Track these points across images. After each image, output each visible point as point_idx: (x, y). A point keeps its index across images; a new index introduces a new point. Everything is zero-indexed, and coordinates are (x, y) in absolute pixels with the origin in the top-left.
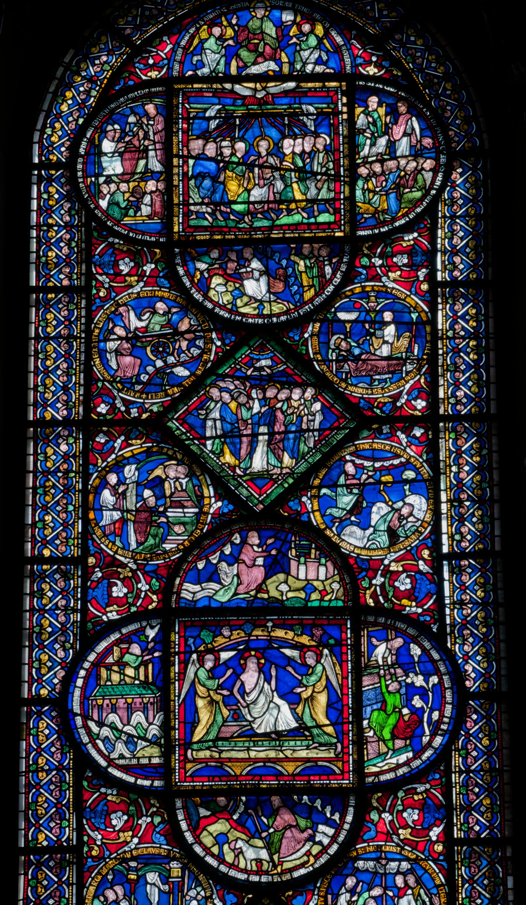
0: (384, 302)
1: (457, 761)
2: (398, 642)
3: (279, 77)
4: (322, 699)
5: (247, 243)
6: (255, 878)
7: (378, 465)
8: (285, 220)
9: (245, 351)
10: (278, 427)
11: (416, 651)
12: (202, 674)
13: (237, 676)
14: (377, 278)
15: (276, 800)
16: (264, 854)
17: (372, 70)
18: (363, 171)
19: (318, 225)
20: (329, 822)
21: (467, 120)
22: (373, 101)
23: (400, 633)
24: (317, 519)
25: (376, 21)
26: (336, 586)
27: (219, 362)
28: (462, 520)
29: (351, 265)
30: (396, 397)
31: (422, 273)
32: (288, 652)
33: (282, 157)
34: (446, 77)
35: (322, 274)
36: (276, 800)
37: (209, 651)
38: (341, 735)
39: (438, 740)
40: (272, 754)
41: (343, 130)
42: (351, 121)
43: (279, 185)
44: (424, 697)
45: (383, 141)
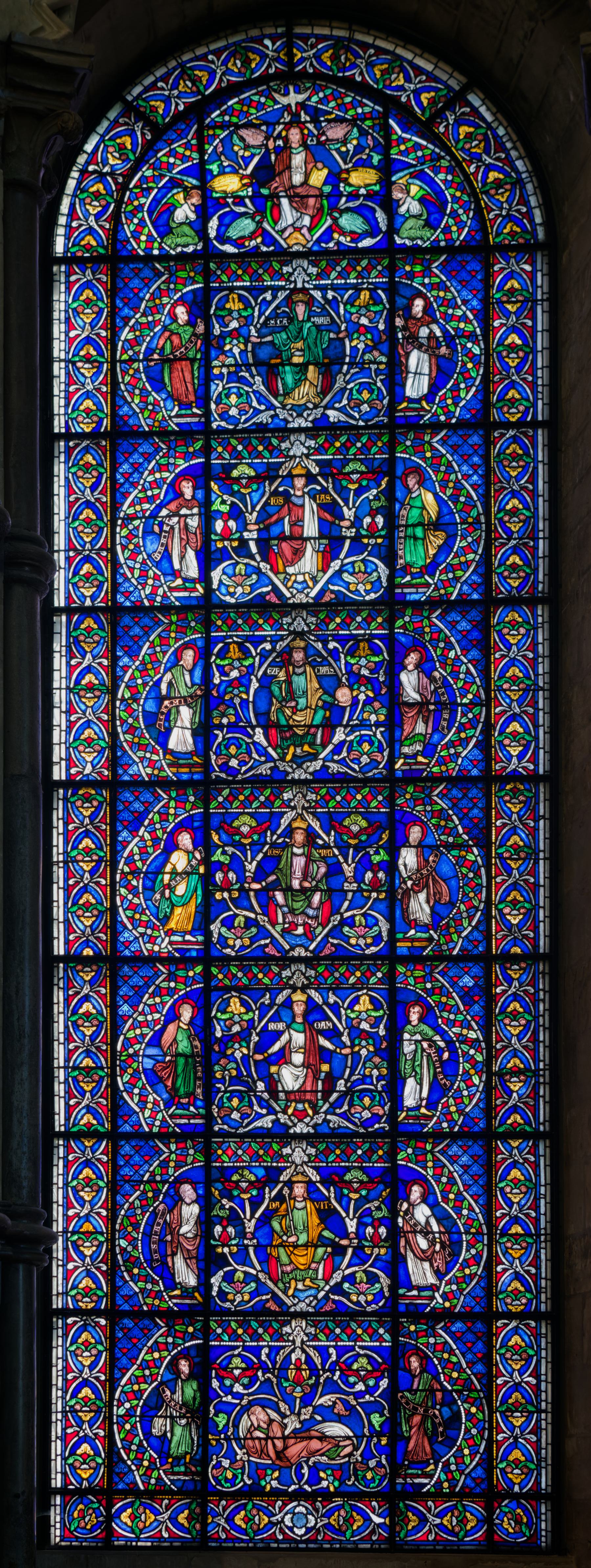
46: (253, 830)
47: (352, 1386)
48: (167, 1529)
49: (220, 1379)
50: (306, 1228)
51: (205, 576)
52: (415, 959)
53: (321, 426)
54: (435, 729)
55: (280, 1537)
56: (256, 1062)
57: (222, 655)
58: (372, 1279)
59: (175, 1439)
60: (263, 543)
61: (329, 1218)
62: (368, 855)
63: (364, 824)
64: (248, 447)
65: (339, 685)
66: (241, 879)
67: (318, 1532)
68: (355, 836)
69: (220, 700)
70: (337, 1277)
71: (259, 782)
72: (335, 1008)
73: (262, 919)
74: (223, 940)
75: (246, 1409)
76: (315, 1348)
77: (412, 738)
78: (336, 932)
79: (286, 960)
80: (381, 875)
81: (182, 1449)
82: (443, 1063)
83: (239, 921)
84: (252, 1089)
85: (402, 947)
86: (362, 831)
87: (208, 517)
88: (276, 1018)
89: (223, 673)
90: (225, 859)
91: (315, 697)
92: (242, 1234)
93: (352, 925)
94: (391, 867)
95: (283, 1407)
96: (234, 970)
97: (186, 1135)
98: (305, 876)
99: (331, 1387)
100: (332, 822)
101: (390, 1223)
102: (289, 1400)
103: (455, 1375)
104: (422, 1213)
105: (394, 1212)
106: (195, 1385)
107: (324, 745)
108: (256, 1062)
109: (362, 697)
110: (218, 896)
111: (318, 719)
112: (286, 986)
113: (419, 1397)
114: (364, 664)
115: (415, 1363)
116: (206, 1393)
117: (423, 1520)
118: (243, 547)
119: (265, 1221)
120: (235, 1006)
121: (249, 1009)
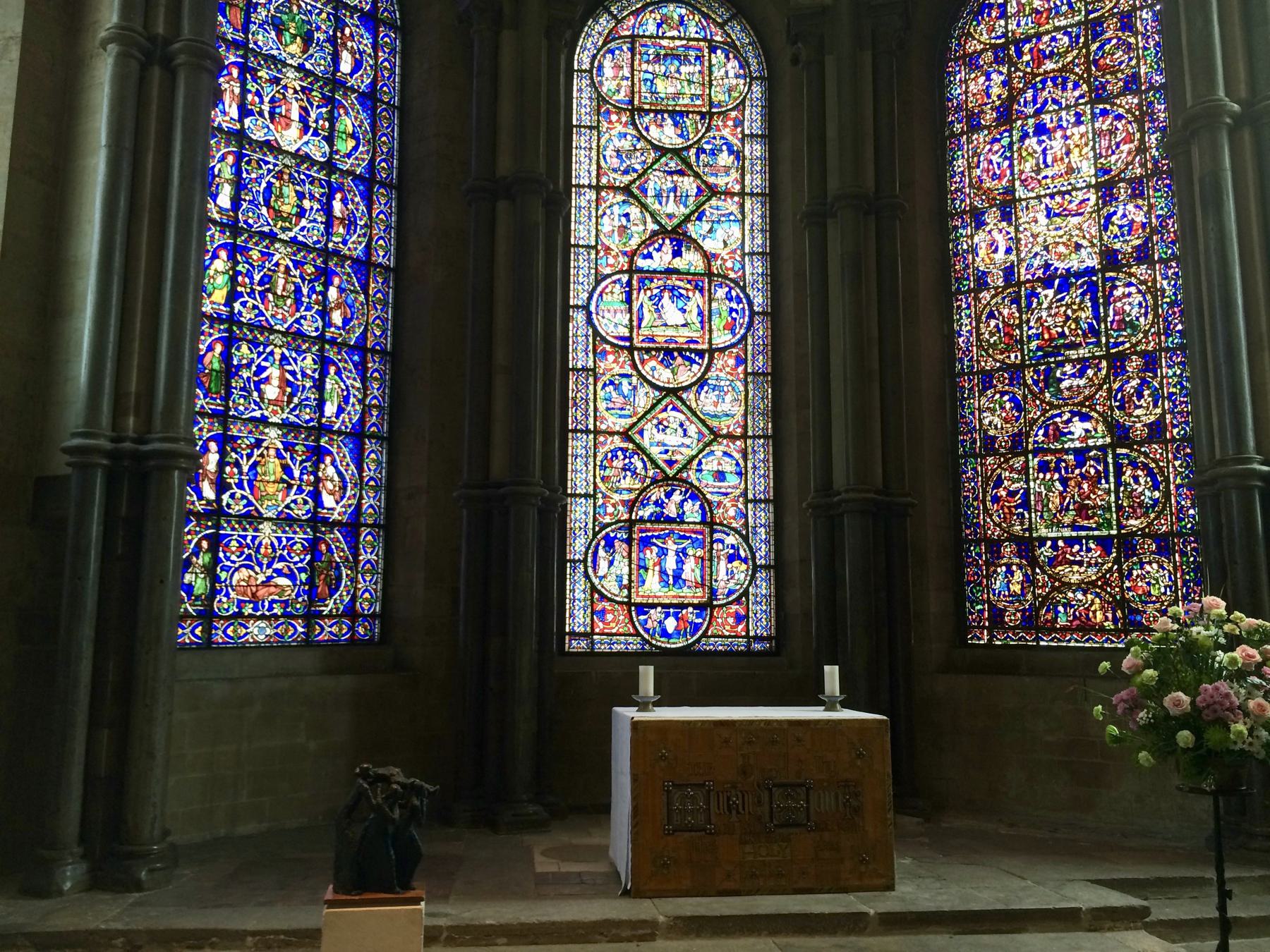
0: (723, 141)
1: (750, 340)
2: (727, 289)
3: (680, 38)
4: (695, 311)
5: (667, 111)
6: (667, 385)
7: (719, 212)
8: (681, 102)
9: (663, 160)
10: (678, 194)
11: (734, 293)
12: (646, 299)
13: (660, 300)
14: (720, 130)
15: (676, 354)
16: (671, 376)
17: (718, 38)
18: (714, 83)
19: (695, 106)
20: (698, 364)
21: (758, 63)
22: (719, 52)
23: (727, 286)
24: (694, 236)
25: (720, 16)
26: (701, 264)
27: (653, 164)
28: (753, 238)
29: (709, 124)
30: (727, 184)
31: (739, 130)
32: (681, 291)
33: (680, 74)
34: (750, 44)
35: (697, 128)
36: (676, 354)
37: (649, 289)
38: (702, 328)
39: (742, 331)
40: (674, 334)
41: (706, 64)
42: (710, 60)
43: (679, 87)
44: (737, 313)
45: (723, 71)
46: (259, 259)
47: (292, 558)
48: (189, 638)
49: (224, 552)
50: (274, 473)
51: (241, 120)
52: (333, 342)
53: (300, 68)
54: (348, 233)
55: (251, 640)
56: (254, 382)
57: (248, 163)
58: (306, 502)
59: (197, 586)
60: (272, 114)
61: (287, 470)
62: (314, 286)
63: (313, 270)
64: (266, 61)
65: (305, 198)
66: (252, 283)
67: (271, 637)
68: (309, 275)
69: (245, 187)
70: (288, 500)
71: (263, 235)
72: (295, 360)
73: (262, 307)
74: (240, 313)
75: (237, 569)
76: (277, 537)
77: (338, 235)
78: (297, 321)
79: (272, 330)
80: (320, 297)
81: (200, 592)
82: (344, 397)
83: (249, 305)
84: (250, 394)
85: (328, 335)
86: (312, 273)
87: (244, 91)
88: (266, 359)
89: (248, 173)
90: (244, 271)
91: (293, 199)
92: (241, 473)
93: (305, 319)
94: (324, 294)
95: (257, 569)
96: (245, 330)
97: (215, 414)
98: (284, 289)
99: (282, 559)
100: (297, 264)
101: (315, 473)
102: (260, 565)
103: (342, 554)
104: (331, 471)
105: (318, 469)
106: (210, 555)
107: (296, 225)
108: (254, 382)
109: (315, 208)
110: (239, 289)
111: (294, 212)
112: (271, 344)
113: (324, 565)
114: (317, 191)
115: (323, 547)
116: (216, 560)
117: (323, 629)
118: (261, 114)
119: (254, 466)
120: (245, 348)
121: (252, 352)
